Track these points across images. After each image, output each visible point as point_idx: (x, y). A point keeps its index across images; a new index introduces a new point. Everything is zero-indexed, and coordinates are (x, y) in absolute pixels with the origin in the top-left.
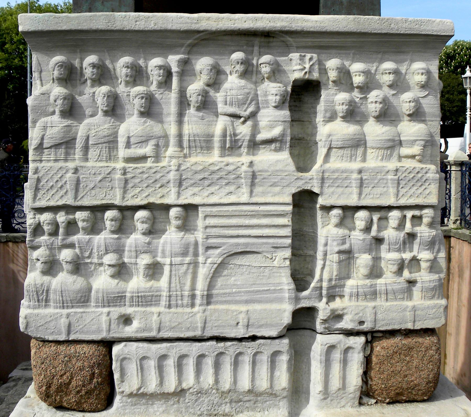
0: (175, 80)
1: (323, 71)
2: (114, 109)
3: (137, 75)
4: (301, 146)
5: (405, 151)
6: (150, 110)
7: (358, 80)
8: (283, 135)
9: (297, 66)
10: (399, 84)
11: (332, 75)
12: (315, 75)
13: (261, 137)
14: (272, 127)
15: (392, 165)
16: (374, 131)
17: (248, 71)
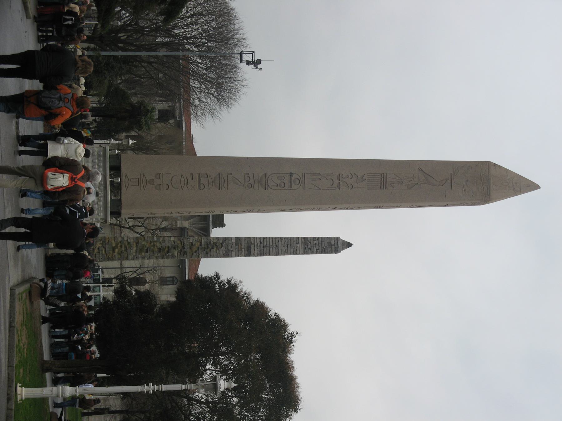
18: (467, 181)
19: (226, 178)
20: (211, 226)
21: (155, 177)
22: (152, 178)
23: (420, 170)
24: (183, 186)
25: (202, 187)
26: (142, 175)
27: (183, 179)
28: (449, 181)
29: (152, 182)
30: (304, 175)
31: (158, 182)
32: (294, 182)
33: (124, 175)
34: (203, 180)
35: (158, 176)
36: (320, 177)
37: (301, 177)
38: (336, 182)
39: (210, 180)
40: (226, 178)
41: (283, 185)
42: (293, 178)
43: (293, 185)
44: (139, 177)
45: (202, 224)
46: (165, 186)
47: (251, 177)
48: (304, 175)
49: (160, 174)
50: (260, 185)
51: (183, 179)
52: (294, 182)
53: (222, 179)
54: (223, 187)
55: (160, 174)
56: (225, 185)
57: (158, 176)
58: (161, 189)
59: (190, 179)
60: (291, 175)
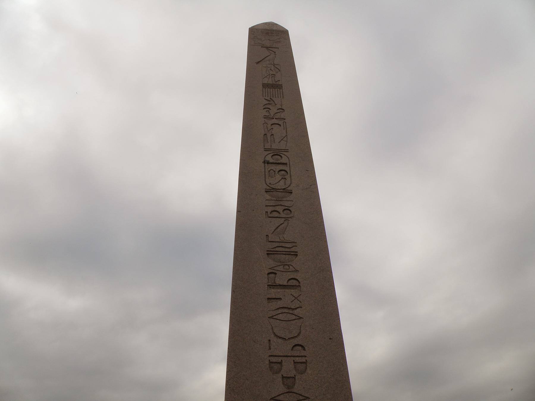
21: (278, 372)
22: (280, 379)
24: (294, 317)
25: (294, 282)
27: (281, 317)
30: (266, 150)
31: (288, 367)
32: (278, 160)
35: (275, 365)
37: (270, 152)
39: (281, 268)
41: (283, 172)
42: (271, 161)
46: (295, 353)
47: (270, 209)
48: (266, 150)
49: (271, 362)
50: (285, 199)
51: (281, 317)
54: (292, 250)
55: (271, 362)
57: (276, 367)
58: (304, 360)
59: (280, 304)
60: (266, 162)
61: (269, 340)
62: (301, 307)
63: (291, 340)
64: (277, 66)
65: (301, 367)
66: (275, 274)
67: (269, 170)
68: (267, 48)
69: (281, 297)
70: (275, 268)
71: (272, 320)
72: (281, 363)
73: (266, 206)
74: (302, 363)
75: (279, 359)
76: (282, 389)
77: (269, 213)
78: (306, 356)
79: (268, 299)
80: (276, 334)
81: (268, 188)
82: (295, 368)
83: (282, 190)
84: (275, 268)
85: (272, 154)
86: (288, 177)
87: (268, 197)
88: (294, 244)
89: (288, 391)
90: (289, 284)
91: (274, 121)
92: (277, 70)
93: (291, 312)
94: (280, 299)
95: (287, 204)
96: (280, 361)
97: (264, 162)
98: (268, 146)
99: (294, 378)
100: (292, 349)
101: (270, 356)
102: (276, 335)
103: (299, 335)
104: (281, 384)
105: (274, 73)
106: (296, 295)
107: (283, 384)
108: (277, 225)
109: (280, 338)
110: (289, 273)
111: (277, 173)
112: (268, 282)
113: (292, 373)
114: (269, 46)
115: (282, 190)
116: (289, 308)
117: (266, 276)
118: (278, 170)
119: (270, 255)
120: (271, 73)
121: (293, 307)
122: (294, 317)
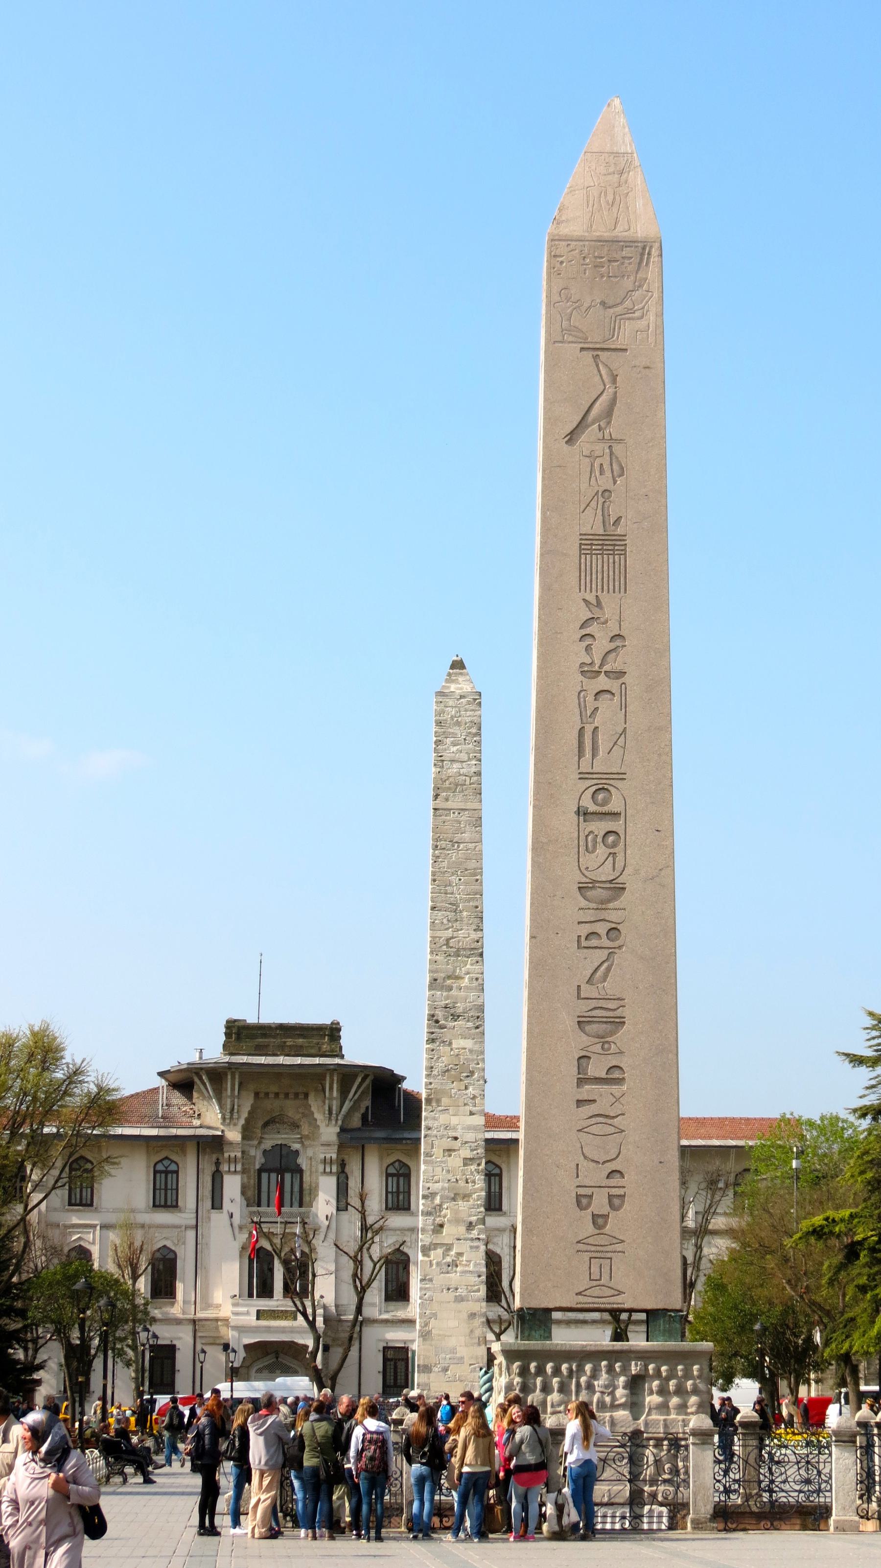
0: (575, 1375)
1: (647, 1369)
2: (546, 1389)
3: (557, 1371)
4: (635, 1406)
5: (689, 1410)
6: (563, 1389)
7: (664, 1374)
8: (626, 1402)
9: (635, 1368)
10: (688, 1375)
11: (651, 1372)
12: (643, 1373)
13: (617, 1403)
14: (621, 1398)
15: (680, 1418)
16: (675, 1401)
17: (610, 1369)
18: (603, 303)
19: (594, 1003)
20: (337, 1061)
21: (586, 1208)
22: (590, 1217)
23: (572, 437)
24: (613, 1130)
25: (616, 1074)
26: (581, 1247)
27: (594, 1129)
28: (603, 355)
29: (599, 1221)
31: (600, 1204)
33: (581, 1299)
34: (595, 1069)
35: (582, 1201)
36: (589, 729)
37: (589, 783)
38: (603, 682)
40: (594, 1003)
41: (611, 839)
42: (592, 808)
43: (611, 807)
44: (586, 1256)
45: (331, 1088)
47: (585, 930)
50: (611, 905)
51: (594, 1129)
52: (605, 802)
53: (594, 1013)
54: (618, 1013)
55: (578, 1197)
56: (611, 1005)
58: (620, 1192)
59: (592, 1109)
60: (583, 813)
61: (578, 1165)
62: (623, 1114)
63: (607, 1164)
64: (617, 448)
65: (616, 1202)
66: (589, 1058)
67: (586, 833)
68: (596, 351)
69: (596, 1098)
70: (589, 1049)
71: (581, 1133)
72: (591, 1197)
73: (579, 923)
74: (619, 1196)
75: (587, 1191)
76: (591, 1229)
77: (583, 939)
78: (624, 1187)
79: (578, 1101)
80: (587, 1154)
81: (584, 880)
82: (610, 1201)
83: (608, 885)
84: (589, 1049)
85: (594, 788)
86: (619, 849)
87: (583, 903)
88: (621, 1003)
89: (598, 1231)
90: (609, 1076)
91: (603, 682)
92: (616, 467)
93: (609, 1121)
94: (594, 1101)
95: (613, 916)
96: (590, 1193)
97: (578, 813)
98: (585, 767)
99: (606, 1217)
100: (608, 1177)
101: (578, 1187)
102: (585, 1157)
103: (617, 1157)
104: (591, 1224)
105: (609, 486)
106: (618, 1095)
107: (594, 1223)
108: (596, 964)
109: (593, 1161)
110: (610, 1057)
111: (599, 839)
112: (579, 1073)
113: (606, 1209)
114: (595, 338)
115: (608, 885)
116: (607, 1116)
117: (576, 1063)
118: (602, 833)
119: (582, 1025)
120: (605, 482)
121: (612, 1114)
122: (613, 1130)
